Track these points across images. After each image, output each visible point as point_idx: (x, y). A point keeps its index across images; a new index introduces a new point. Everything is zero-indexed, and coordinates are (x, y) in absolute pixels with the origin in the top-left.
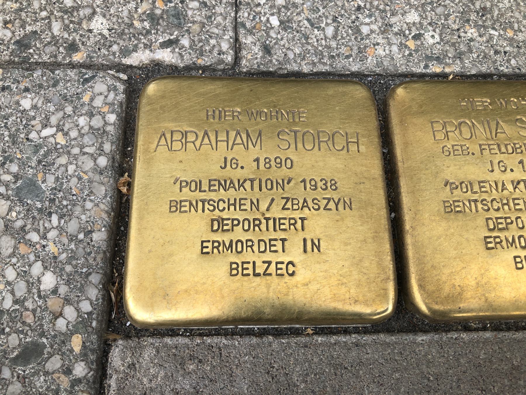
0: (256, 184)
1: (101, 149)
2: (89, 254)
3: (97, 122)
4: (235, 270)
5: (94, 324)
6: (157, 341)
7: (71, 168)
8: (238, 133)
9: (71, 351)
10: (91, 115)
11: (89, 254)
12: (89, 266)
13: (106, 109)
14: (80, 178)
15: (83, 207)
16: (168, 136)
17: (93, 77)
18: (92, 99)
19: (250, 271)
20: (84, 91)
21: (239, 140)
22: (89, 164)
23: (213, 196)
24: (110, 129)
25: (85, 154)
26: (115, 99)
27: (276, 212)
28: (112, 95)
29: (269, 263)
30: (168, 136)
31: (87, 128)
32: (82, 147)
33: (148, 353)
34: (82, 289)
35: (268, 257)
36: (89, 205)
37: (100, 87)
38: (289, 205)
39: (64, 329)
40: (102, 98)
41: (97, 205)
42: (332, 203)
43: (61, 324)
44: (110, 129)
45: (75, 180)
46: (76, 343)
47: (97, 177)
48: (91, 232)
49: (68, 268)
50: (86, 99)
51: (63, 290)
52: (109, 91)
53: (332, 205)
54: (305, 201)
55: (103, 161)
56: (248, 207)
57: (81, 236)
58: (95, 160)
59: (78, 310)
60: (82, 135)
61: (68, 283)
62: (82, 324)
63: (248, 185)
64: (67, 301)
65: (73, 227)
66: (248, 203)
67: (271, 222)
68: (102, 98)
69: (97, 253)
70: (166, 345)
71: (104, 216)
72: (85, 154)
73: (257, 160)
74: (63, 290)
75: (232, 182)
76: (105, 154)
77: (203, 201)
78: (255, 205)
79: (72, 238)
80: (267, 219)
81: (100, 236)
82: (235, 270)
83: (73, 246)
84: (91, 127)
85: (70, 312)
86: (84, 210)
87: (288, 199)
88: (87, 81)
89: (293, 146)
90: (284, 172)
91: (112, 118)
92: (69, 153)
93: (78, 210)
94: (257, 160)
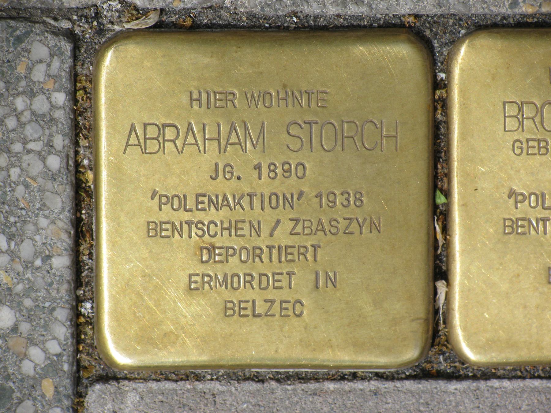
0: (256, 203)
1: (49, 145)
2: (50, 284)
3: (40, 104)
4: (229, 310)
5: (66, 367)
6: (141, 386)
7: (15, 172)
8: (233, 128)
9: (43, 396)
10: (32, 94)
11: (50, 284)
12: (53, 300)
13: (50, 85)
14: (27, 186)
15: (36, 224)
16: (140, 131)
17: (27, 34)
18: (30, 69)
19: (249, 312)
20: (18, 56)
21: (234, 139)
22: (37, 167)
23: (200, 216)
24: (59, 114)
25: (29, 152)
26: (61, 69)
27: (282, 237)
28: (56, 63)
29: (272, 302)
30: (140, 131)
31: (27, 114)
32: (25, 142)
33: (132, 398)
34: (46, 327)
35: (271, 294)
36: (43, 222)
37: (40, 50)
38: (299, 229)
39: (32, 373)
40: (42, 67)
41: (53, 222)
42: (355, 224)
43: (27, 368)
44: (59, 114)
45: (20, 189)
46: (48, 387)
47: (49, 185)
48: (49, 257)
49: (28, 303)
50: (21, 69)
51: (25, 327)
52: (52, 56)
53: (354, 227)
54: (320, 222)
55: (54, 162)
56: (246, 232)
57: (38, 262)
58: (44, 160)
59: (45, 351)
60: (22, 125)
61: (29, 319)
62: (51, 367)
63: (245, 202)
64: (31, 341)
65: (26, 250)
66: (246, 226)
67: (275, 252)
68: (42, 67)
69: (60, 283)
70: (150, 391)
71: (64, 236)
72: (29, 152)
73: (258, 167)
74: (25, 327)
75: (225, 198)
76: (57, 153)
77: (189, 223)
78: (255, 228)
79: (28, 265)
80: (270, 248)
81: (61, 262)
82: (229, 310)
83: (29, 275)
84: (33, 113)
85: (36, 353)
86: (38, 229)
87: (297, 221)
88: (19, 40)
89: (306, 146)
90: (293, 184)
91: (60, 98)
92: (9, 151)
93: (30, 228)
94: (258, 167)
